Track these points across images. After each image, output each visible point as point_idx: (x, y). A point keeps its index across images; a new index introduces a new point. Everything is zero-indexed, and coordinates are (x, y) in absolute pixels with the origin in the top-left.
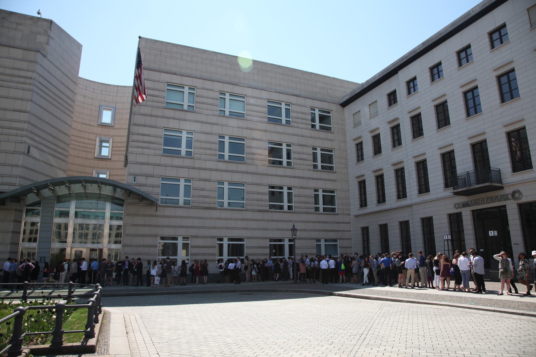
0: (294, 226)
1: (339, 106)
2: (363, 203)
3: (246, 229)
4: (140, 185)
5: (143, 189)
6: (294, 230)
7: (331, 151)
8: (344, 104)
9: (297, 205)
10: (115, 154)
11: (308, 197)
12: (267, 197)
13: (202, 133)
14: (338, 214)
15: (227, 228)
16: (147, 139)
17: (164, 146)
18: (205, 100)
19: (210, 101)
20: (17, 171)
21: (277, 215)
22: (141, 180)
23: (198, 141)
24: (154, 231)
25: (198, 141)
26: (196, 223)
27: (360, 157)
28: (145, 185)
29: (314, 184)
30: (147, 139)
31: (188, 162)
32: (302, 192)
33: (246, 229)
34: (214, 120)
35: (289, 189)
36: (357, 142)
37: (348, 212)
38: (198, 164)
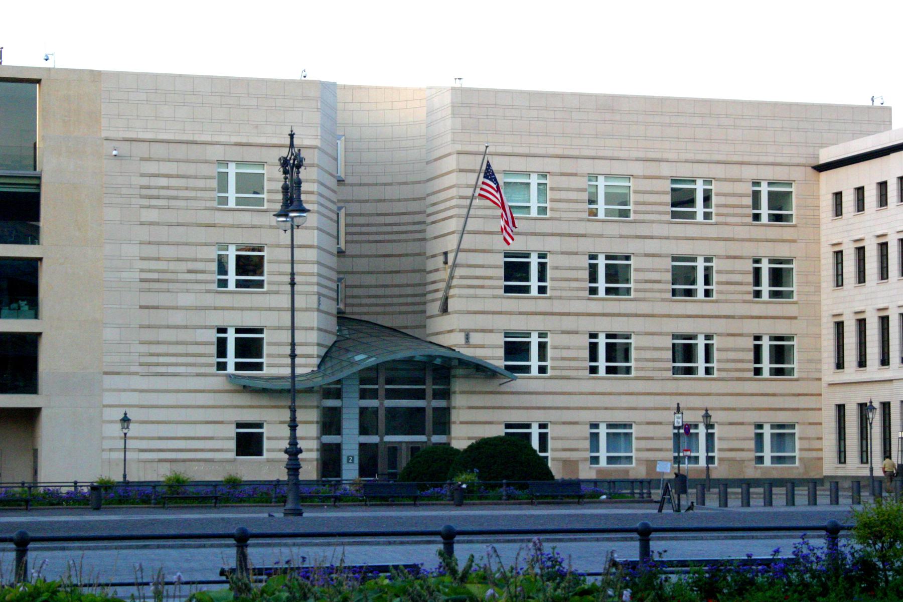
1: (810, 170)
2: (840, 365)
4: (476, 346)
8: (821, 168)
10: (352, 242)
13: (563, 253)
14: (797, 380)
17: (506, 280)
23: (557, 268)
25: (557, 268)
27: (839, 280)
28: (482, 346)
29: (755, 327)
31: (543, 305)
32: (730, 342)
34: (580, 228)
35: (708, 337)
36: (837, 249)
37: (816, 375)
38: (558, 306)
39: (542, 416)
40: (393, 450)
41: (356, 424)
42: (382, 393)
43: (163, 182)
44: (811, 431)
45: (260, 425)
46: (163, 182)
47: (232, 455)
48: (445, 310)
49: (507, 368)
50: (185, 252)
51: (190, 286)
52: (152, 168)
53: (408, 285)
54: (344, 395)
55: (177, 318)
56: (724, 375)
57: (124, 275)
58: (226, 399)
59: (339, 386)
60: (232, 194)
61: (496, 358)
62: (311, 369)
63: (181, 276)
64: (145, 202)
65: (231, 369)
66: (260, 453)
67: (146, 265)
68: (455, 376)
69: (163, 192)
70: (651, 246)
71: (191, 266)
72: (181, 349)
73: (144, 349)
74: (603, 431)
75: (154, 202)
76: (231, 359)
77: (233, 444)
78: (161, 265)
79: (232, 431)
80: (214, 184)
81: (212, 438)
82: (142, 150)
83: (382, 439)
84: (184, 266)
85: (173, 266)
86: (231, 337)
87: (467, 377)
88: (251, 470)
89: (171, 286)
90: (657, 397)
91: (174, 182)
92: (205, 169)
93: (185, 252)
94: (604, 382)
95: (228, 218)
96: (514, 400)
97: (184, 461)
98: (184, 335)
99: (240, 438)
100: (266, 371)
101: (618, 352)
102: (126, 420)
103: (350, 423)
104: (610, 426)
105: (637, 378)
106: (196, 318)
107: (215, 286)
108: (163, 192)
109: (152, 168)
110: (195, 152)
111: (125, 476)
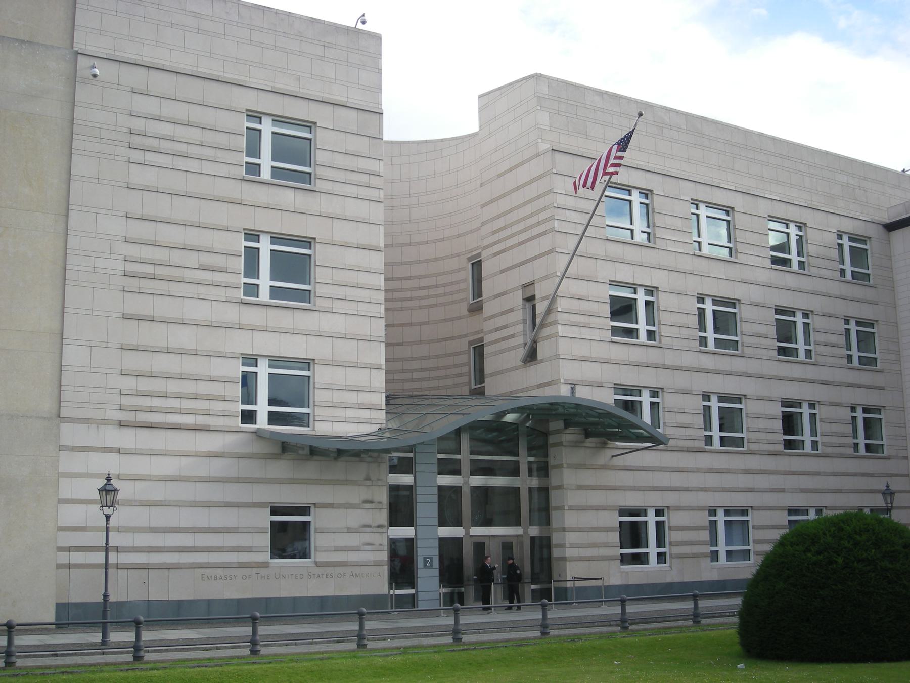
0: (888, 486)
3: (752, 490)
6: (888, 493)
7: (871, 325)
9: (827, 440)
11: (841, 422)
12: (778, 425)
14: (888, 458)
15: (724, 490)
21: (793, 462)
22: (584, 393)
24: (596, 498)
26: (676, 480)
31: (653, 355)
33: (752, 490)
38: (670, 358)
39: (656, 499)
40: (480, 547)
41: (434, 510)
42: (466, 467)
43: (166, 129)
45: (304, 510)
46: (166, 129)
47: (266, 556)
48: (532, 356)
50: (194, 237)
51: (202, 290)
52: (149, 106)
53: (413, 359)
54: (419, 468)
55: (184, 338)
56: (829, 450)
57: (100, 263)
58: (253, 469)
59: (411, 455)
60: (266, 162)
62: (379, 426)
63: (189, 274)
64: (137, 156)
65: (262, 421)
66: (305, 555)
67: (133, 251)
68: (559, 444)
69: (165, 145)
71: (207, 259)
72: (188, 387)
73: (129, 383)
75: (150, 157)
77: (265, 540)
78: (159, 254)
79: (265, 519)
80: (242, 142)
81: (234, 530)
82: (137, 77)
83: (467, 533)
84: (193, 259)
85: (176, 257)
86: (263, 371)
87: (576, 444)
88: (292, 579)
89: (176, 289)
90: (772, 476)
91: (181, 132)
92: (227, 120)
93: (194, 237)
95: (260, 194)
96: (626, 478)
97: (192, 566)
98: (190, 365)
99: (278, 529)
102: (108, 490)
103: (426, 507)
104: (727, 512)
105: (751, 453)
106: (212, 341)
108: (165, 145)
109: (149, 106)
110: (215, 93)
111: (106, 596)
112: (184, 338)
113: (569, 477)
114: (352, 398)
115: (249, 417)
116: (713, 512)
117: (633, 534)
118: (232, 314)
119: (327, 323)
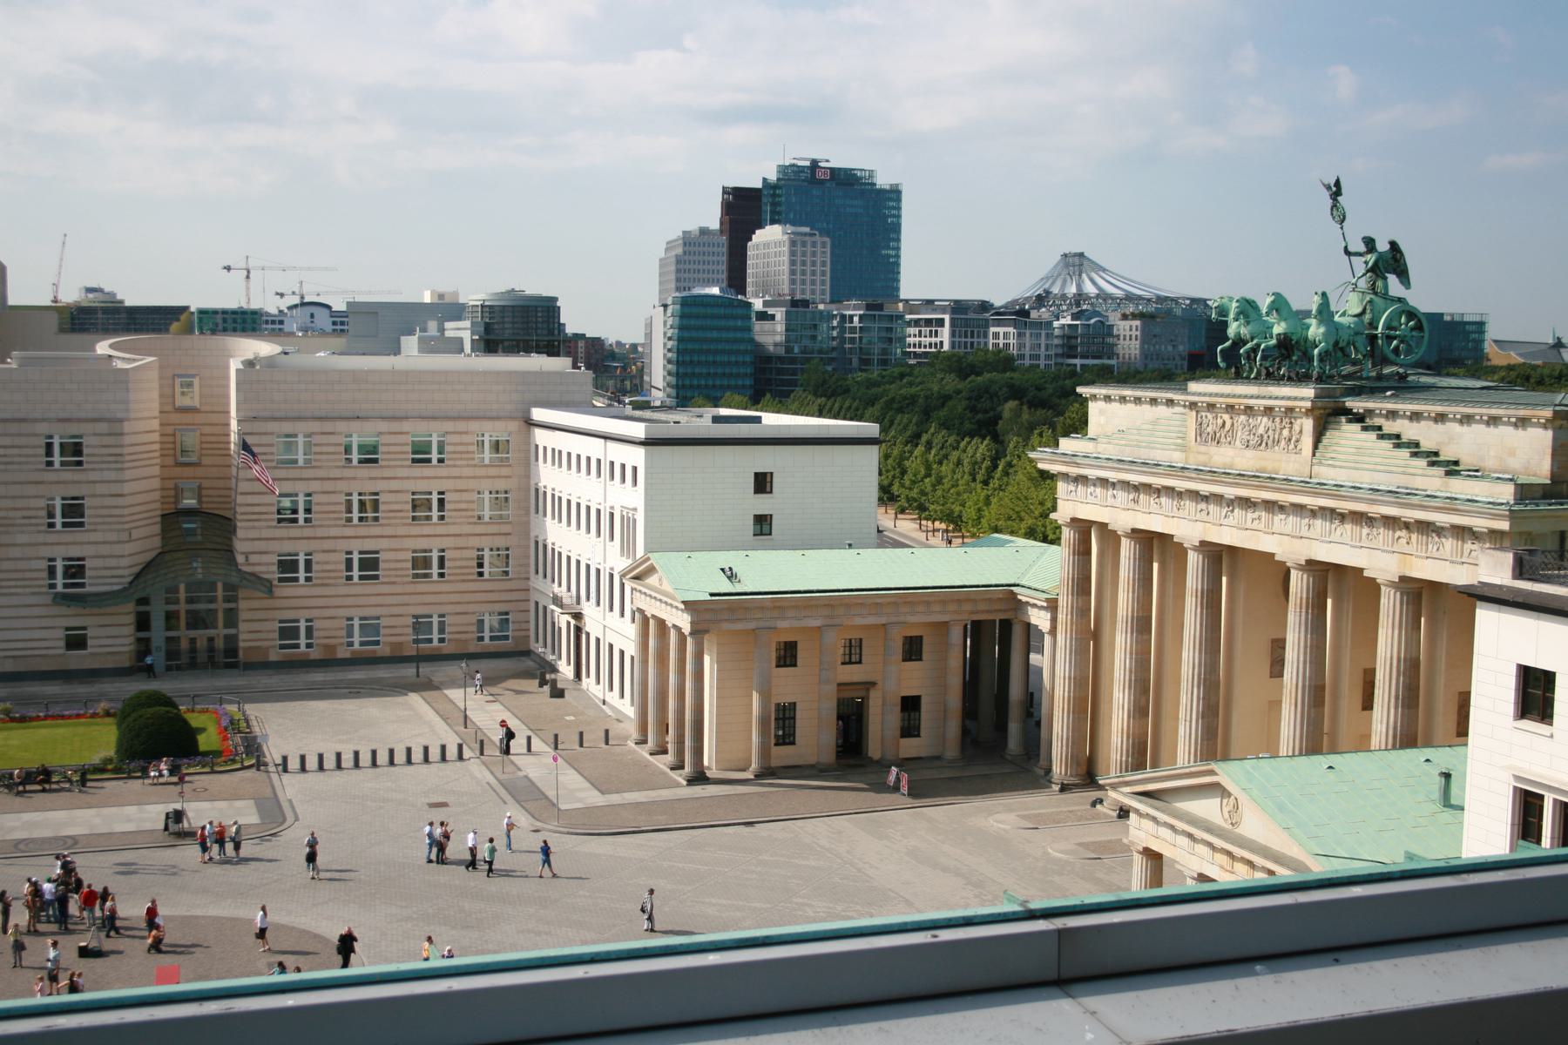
5: (257, 569)
16: (257, 509)
18: (325, 449)
19: (331, 449)
20: (124, 562)
30: (257, 509)
31: (307, 532)
38: (319, 532)
44: (521, 617)
45: (84, 628)
47: (62, 651)
49: (281, 580)
55: (16, 552)
61: (273, 573)
70: (394, 485)
74: (356, 623)
76: (60, 581)
77: (62, 643)
79: (61, 634)
84: (19, 514)
85: (11, 514)
93: (20, 503)
94: (358, 587)
100: (88, 589)
101: (370, 564)
103: (158, 622)
107: (44, 528)
110: (26, 428)
112: (16, 552)
113: (243, 604)
114: (108, 573)
115: (53, 586)
116: (351, 619)
117: (288, 632)
118: (41, 538)
119: (93, 537)
